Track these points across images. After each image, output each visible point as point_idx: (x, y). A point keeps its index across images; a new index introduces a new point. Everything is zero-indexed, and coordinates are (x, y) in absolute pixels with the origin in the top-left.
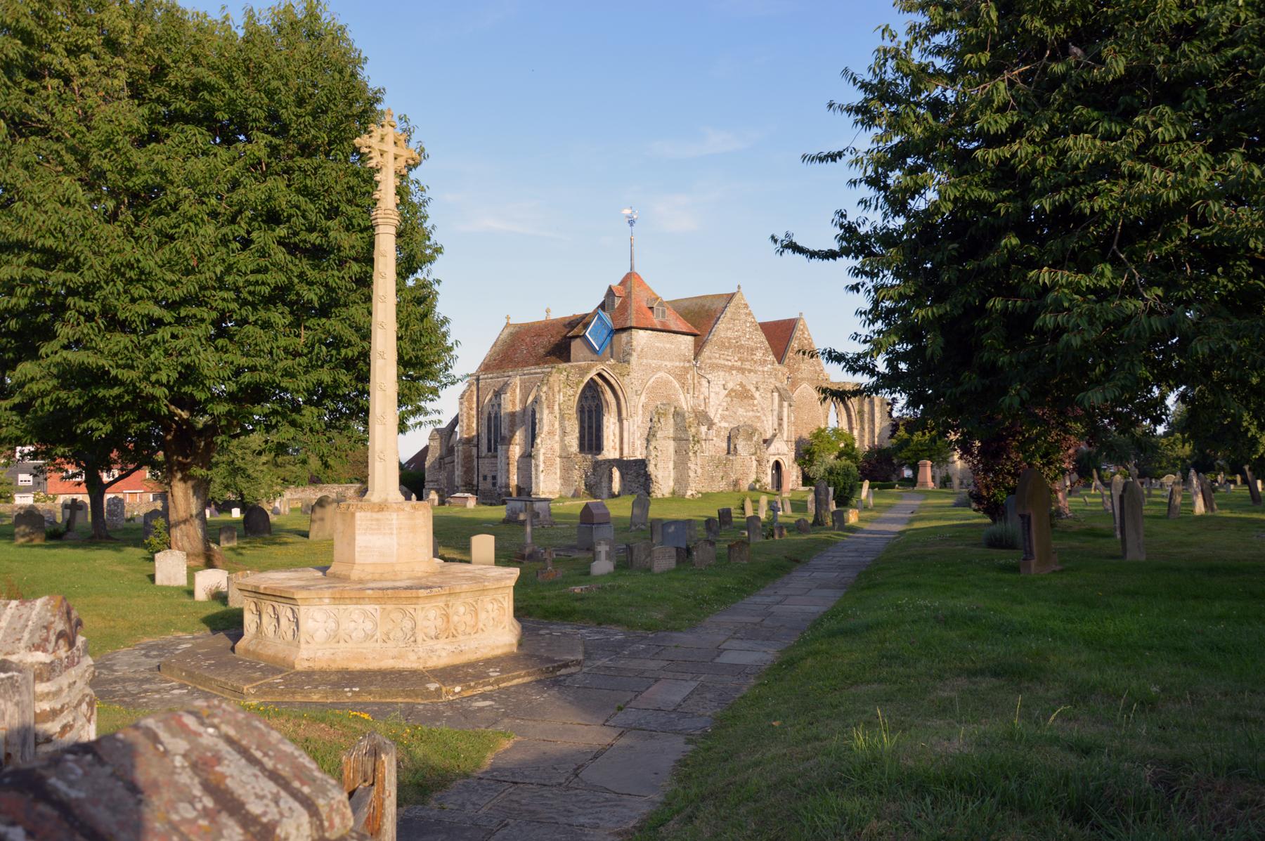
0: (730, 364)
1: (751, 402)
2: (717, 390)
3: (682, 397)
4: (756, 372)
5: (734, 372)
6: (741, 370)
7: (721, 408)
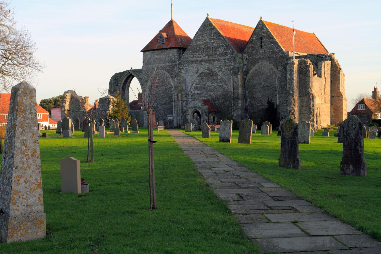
0: (200, 59)
1: (215, 78)
2: (192, 74)
3: (170, 80)
4: (219, 60)
5: (203, 63)
6: (209, 61)
7: (195, 83)
